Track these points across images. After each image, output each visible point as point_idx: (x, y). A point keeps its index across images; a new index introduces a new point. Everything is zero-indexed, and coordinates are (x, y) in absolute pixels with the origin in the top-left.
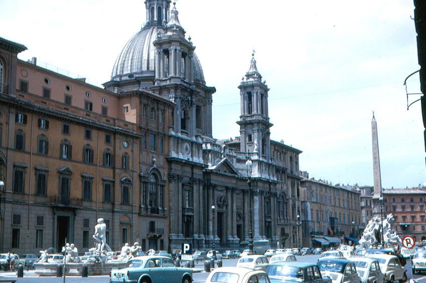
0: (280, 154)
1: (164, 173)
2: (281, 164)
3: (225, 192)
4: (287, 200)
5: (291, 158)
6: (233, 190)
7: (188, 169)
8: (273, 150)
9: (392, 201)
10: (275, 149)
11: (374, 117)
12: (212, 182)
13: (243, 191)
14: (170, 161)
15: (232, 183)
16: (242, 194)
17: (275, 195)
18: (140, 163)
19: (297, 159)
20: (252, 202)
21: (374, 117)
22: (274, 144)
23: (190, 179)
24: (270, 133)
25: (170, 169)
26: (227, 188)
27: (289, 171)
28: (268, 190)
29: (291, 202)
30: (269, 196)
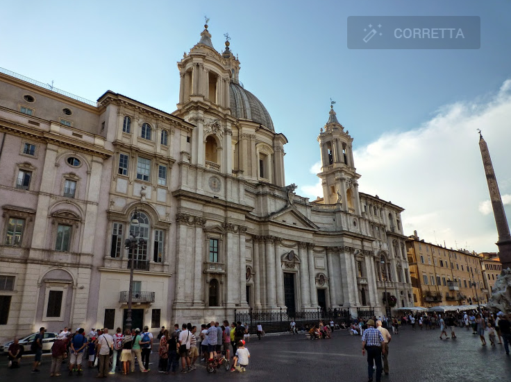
1: (165, 211)
2: (376, 221)
3: (296, 247)
4: (389, 260)
5: (390, 215)
6: (308, 246)
7: (220, 212)
8: (363, 204)
10: (367, 204)
11: (481, 137)
12: (271, 234)
13: (326, 249)
14: (179, 195)
15: (308, 237)
16: (325, 252)
17: (370, 253)
18: (110, 194)
19: (399, 217)
20: (340, 263)
21: (481, 137)
22: (363, 196)
23: (222, 224)
24: (358, 185)
25: (179, 208)
26: (299, 244)
27: (388, 229)
29: (394, 264)
30: (361, 254)
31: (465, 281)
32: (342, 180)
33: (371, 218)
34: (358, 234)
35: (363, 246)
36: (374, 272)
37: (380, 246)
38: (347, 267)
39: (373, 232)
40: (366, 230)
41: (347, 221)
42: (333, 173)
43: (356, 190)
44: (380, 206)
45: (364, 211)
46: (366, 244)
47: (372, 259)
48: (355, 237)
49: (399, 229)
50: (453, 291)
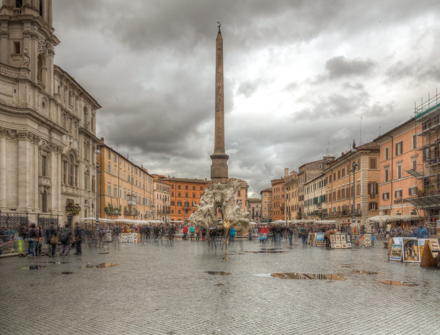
0: (70, 96)
4: (78, 162)
5: (85, 109)
8: (57, 83)
9: (177, 188)
10: (61, 84)
17: (59, 149)
19: (94, 115)
27: (82, 124)
28: (47, 138)
30: (47, 147)
31: (140, 197)
32: (33, 36)
33: (64, 105)
34: (48, 120)
35: (51, 138)
36: (60, 173)
37: (70, 143)
38: (28, 161)
39: (65, 123)
40: (57, 118)
41: (34, 98)
42: (21, 23)
43: (50, 61)
44: (76, 93)
45: (56, 92)
46: (55, 136)
47: (60, 156)
48: (43, 123)
49: (92, 128)
50: (130, 206)
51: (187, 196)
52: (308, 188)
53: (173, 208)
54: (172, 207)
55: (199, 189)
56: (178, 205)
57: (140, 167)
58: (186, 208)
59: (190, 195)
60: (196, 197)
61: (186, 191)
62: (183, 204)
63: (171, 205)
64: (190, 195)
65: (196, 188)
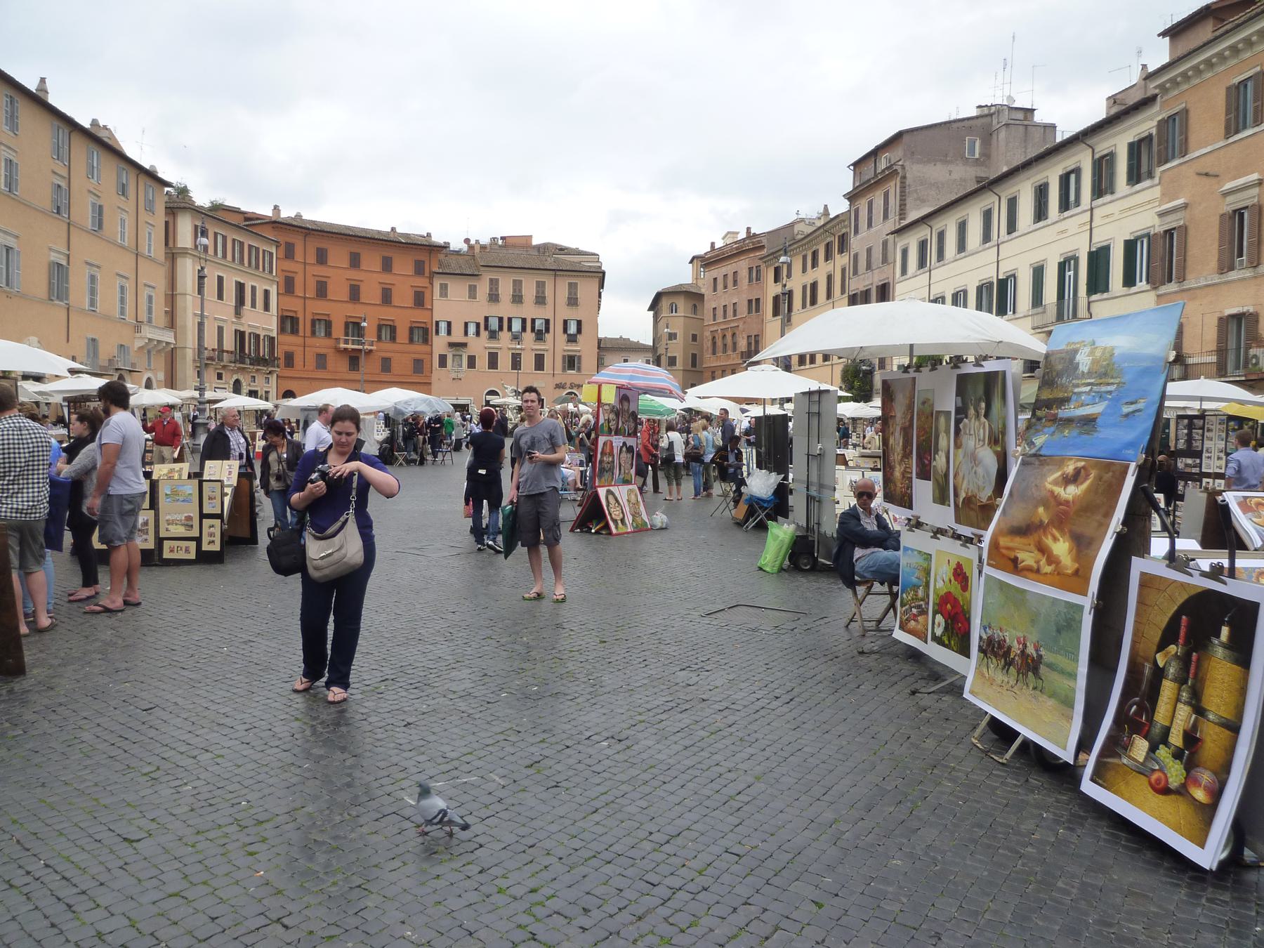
9: (312, 259)
51: (355, 294)
52: (1064, 180)
53: (288, 343)
54: (289, 338)
55: (410, 270)
56: (313, 333)
57: (32, 86)
58: (350, 346)
59: (371, 293)
60: (396, 300)
61: (354, 275)
62: (338, 331)
63: (282, 330)
64: (371, 293)
65: (397, 268)
